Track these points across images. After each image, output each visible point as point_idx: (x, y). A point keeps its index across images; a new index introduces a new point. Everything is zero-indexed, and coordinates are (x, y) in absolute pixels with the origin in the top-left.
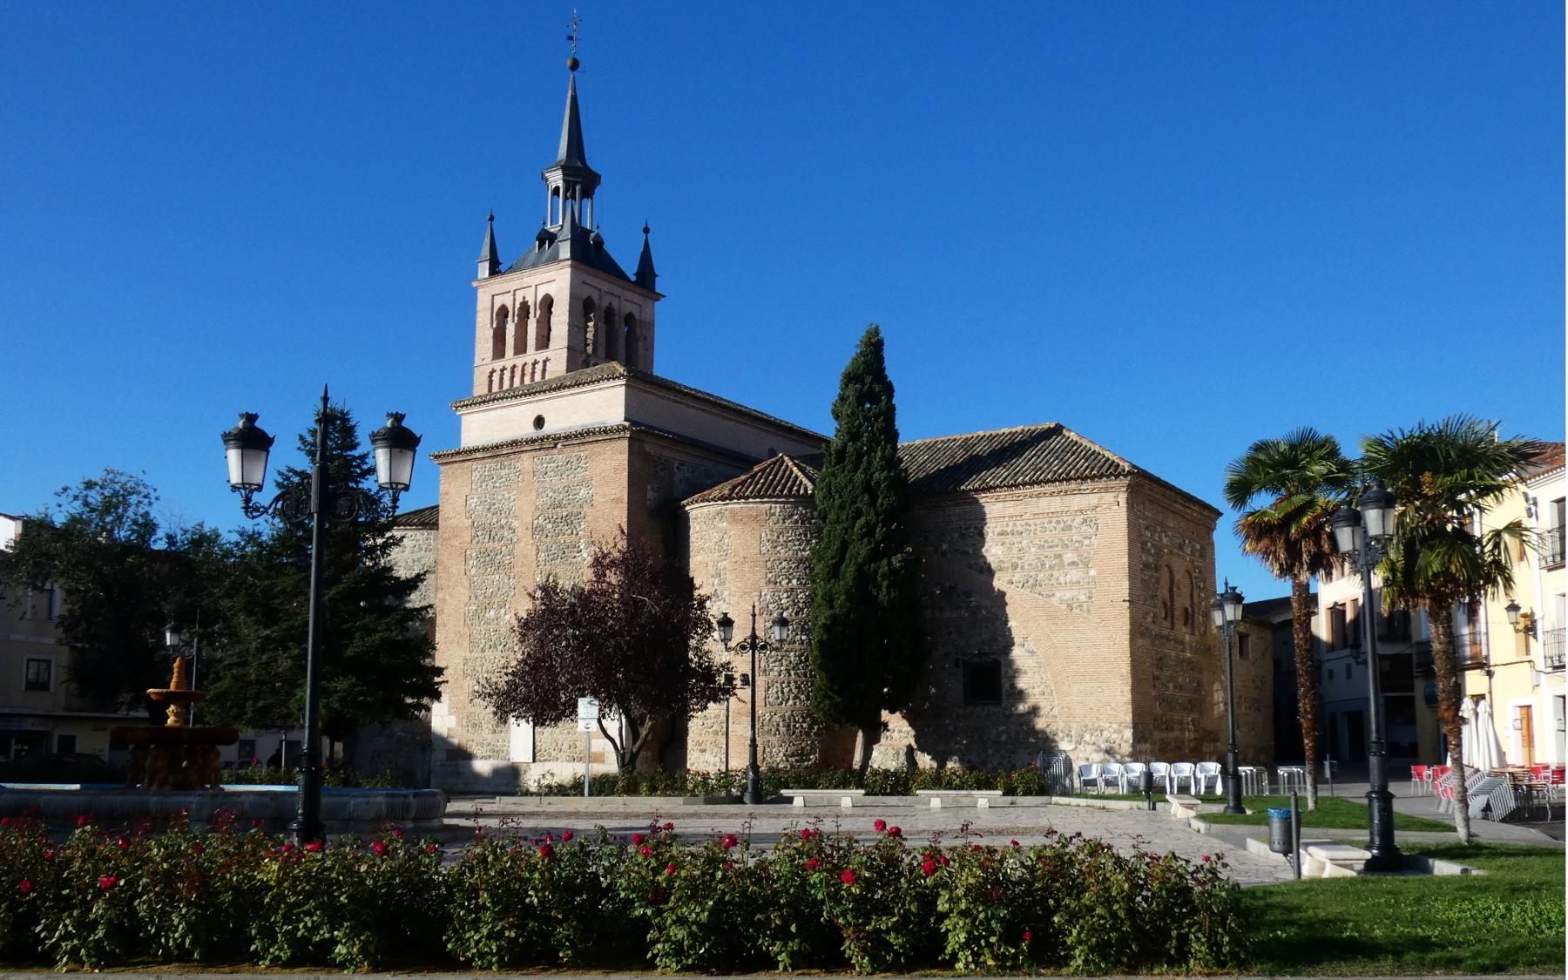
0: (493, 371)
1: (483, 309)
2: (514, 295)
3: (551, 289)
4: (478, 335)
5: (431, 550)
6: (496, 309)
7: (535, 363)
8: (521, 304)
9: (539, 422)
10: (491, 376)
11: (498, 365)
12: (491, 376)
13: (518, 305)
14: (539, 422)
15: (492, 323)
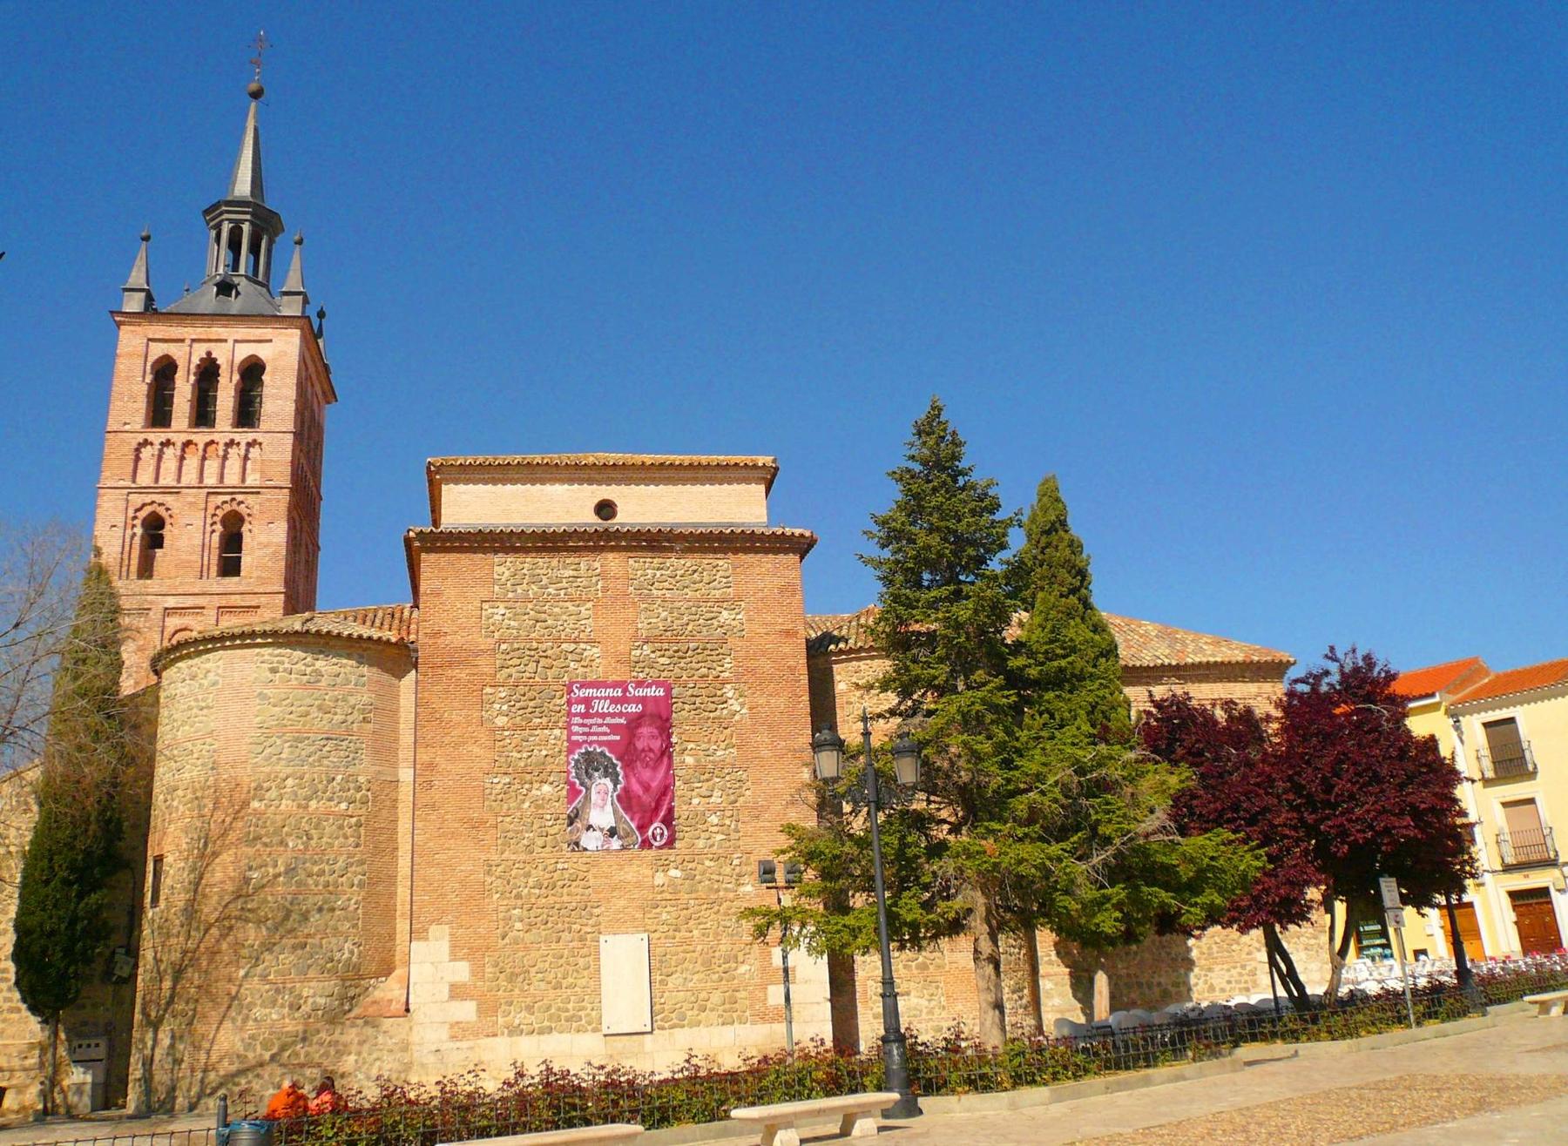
0: (146, 443)
1: (130, 355)
2: (191, 346)
3: (263, 352)
4: (118, 386)
5: (364, 685)
6: (151, 359)
7: (231, 443)
8: (202, 360)
9: (605, 509)
10: (138, 450)
11: (157, 436)
12: (138, 450)
13: (196, 361)
14: (605, 509)
15: (144, 377)
